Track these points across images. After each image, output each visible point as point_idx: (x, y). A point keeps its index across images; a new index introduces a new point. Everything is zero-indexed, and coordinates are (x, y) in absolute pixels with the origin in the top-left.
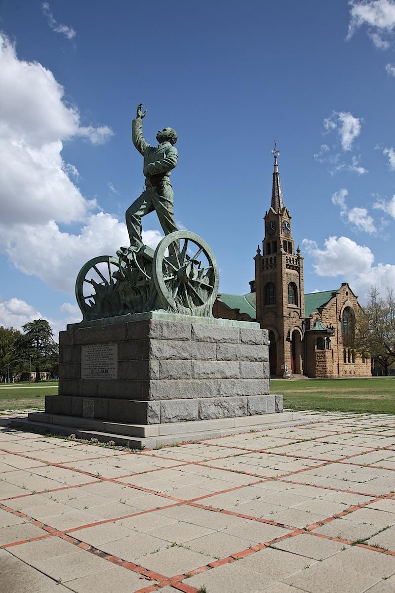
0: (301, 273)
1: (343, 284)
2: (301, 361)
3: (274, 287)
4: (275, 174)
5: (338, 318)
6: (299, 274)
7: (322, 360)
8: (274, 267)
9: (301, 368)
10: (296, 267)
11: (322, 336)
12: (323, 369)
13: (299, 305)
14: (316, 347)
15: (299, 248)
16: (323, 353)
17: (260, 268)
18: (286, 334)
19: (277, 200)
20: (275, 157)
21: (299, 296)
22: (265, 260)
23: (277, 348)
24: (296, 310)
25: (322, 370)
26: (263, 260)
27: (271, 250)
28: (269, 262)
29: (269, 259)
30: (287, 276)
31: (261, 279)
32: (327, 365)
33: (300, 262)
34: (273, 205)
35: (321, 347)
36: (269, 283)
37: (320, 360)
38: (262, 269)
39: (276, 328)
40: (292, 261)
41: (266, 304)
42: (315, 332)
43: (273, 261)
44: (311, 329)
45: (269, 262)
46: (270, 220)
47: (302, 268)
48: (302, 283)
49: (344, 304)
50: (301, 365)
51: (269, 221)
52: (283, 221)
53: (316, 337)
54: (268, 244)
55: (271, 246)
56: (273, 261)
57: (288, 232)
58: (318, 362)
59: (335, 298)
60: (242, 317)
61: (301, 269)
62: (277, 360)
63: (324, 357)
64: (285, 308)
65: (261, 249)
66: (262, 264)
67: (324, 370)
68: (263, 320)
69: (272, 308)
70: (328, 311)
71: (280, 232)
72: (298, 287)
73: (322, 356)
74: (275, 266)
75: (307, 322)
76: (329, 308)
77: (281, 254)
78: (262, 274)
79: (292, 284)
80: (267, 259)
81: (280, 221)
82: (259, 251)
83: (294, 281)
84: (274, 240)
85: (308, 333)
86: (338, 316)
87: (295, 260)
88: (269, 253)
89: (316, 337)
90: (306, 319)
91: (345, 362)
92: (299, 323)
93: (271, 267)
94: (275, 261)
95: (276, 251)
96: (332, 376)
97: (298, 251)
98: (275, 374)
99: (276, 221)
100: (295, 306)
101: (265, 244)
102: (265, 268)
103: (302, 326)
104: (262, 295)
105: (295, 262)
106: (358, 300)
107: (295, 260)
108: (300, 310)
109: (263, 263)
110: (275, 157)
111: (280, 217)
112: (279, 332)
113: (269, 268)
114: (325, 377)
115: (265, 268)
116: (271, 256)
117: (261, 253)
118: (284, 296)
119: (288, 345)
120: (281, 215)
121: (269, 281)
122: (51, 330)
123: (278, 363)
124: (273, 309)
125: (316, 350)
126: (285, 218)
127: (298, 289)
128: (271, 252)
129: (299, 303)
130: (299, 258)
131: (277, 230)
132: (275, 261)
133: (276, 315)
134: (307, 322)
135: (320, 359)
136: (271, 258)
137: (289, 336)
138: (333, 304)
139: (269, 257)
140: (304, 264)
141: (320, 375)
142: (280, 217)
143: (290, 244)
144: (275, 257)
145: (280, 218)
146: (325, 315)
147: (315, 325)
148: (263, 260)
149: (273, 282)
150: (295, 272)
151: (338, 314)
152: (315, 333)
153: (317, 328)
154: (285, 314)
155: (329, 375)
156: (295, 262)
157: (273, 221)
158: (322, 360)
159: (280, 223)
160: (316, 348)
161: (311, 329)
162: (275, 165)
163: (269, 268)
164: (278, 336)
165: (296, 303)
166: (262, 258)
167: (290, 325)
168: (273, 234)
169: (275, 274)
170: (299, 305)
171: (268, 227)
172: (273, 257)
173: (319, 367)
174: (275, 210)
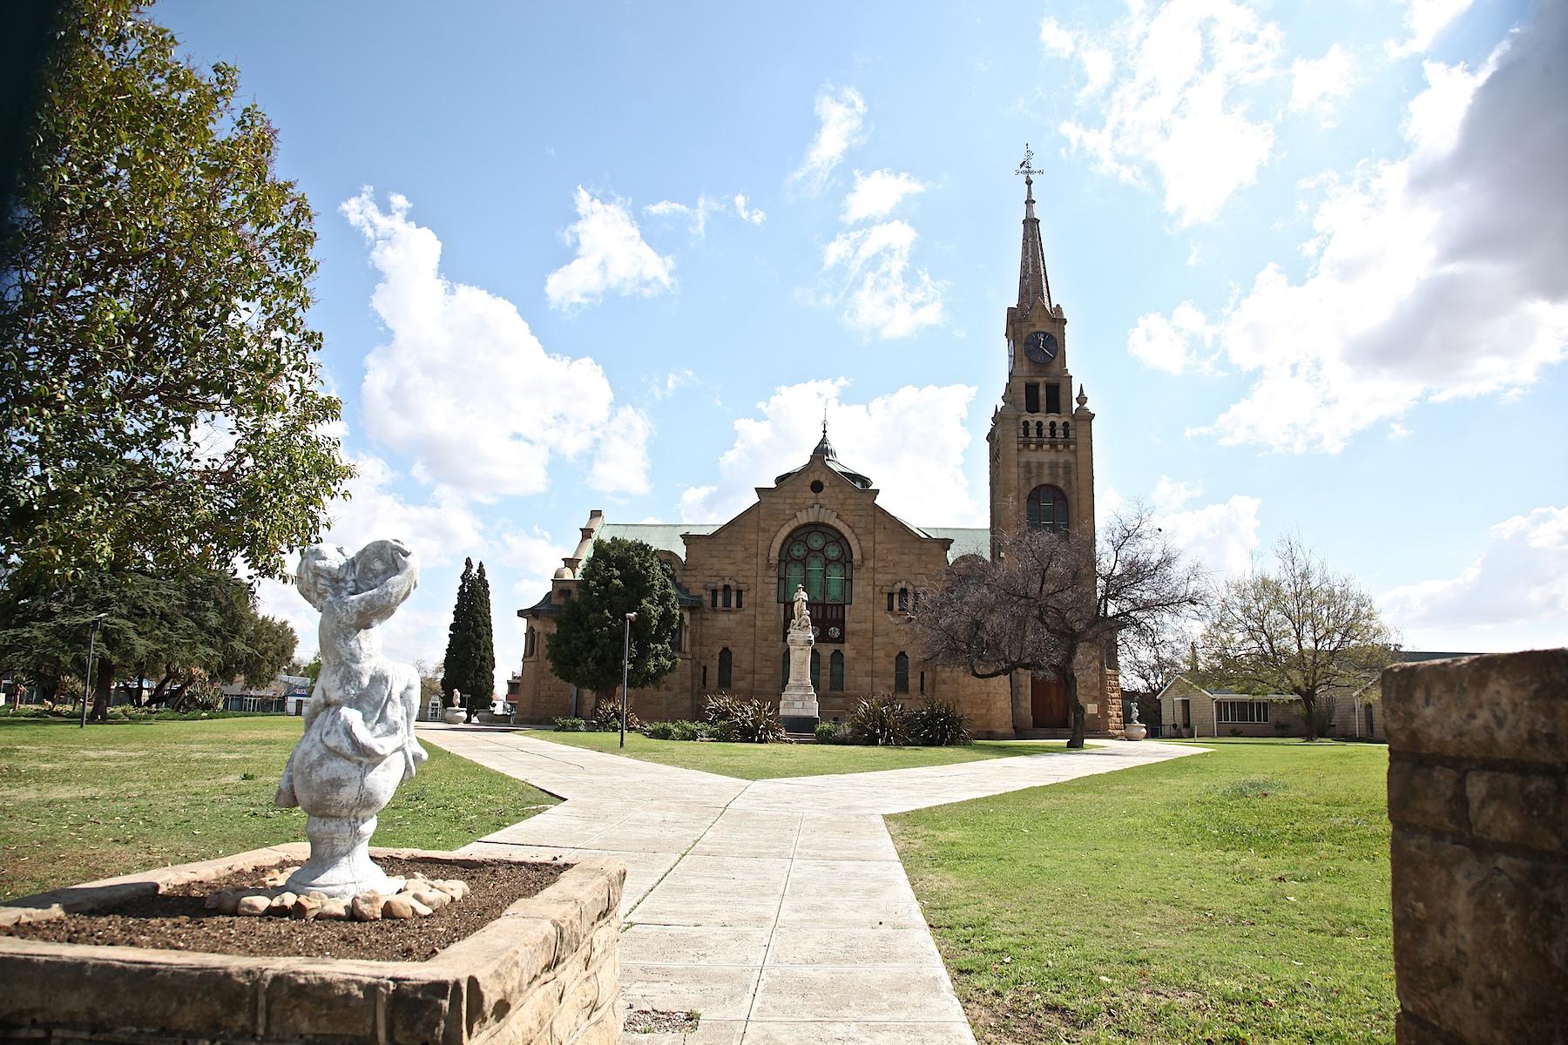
8: (1060, 447)
22: (1033, 425)
27: (1043, 403)
28: (1046, 432)
31: (1022, 471)
38: (1021, 446)
43: (1060, 433)
45: (1046, 432)
46: (1037, 329)
54: (1031, 389)
55: (1042, 392)
56: (1060, 433)
74: (1067, 446)
80: (1053, 424)
84: (1051, 380)
88: (1033, 407)
94: (1066, 434)
99: (1056, 336)
109: (1026, 433)
115: (1032, 446)
121: (1046, 480)
131: (1058, 358)
132: (1066, 434)
144: (1066, 424)
149: (1061, 484)
157: (1045, 334)
163: (1046, 447)
172: (1046, 423)
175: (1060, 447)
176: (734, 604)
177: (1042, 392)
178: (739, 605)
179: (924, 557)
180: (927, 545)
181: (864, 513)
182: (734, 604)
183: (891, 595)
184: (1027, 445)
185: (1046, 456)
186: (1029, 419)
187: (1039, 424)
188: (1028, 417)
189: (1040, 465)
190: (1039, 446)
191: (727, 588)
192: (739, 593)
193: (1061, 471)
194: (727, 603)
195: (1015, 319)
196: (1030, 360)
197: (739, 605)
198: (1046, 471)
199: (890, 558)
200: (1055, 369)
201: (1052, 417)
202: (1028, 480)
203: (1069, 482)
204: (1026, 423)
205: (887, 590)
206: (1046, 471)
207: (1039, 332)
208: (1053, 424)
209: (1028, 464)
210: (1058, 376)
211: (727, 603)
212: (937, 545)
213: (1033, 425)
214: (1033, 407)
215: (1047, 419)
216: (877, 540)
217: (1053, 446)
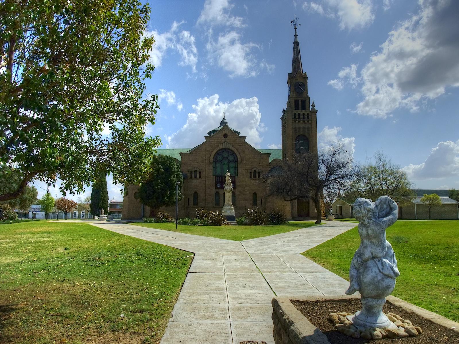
4: (296, 44)
17: (292, 120)
22: (297, 114)
27: (300, 106)
28: (302, 117)
38: (293, 121)
43: (306, 117)
45: (302, 117)
46: (298, 81)
51: (297, 81)
54: (296, 102)
55: (300, 103)
56: (306, 117)
66: (293, 116)
74: (308, 121)
80: (304, 114)
109: (295, 117)
115: (297, 122)
116: (298, 112)
121: (302, 133)
149: (306, 134)
163: (302, 122)
175: (306, 122)
176: (198, 176)
177: (300, 103)
178: (200, 177)
180: (263, 156)
182: (198, 176)
183: (251, 173)
184: (295, 121)
185: (302, 125)
186: (296, 112)
187: (299, 114)
188: (296, 112)
189: (299, 128)
190: (299, 121)
191: (196, 171)
192: (200, 173)
193: (306, 130)
194: (196, 176)
195: (291, 78)
196: (296, 92)
197: (200, 177)
199: (250, 160)
201: (303, 112)
204: (295, 114)
205: (249, 171)
207: (299, 82)
208: (304, 114)
211: (196, 176)
213: (297, 114)
214: (297, 108)
215: (302, 112)
217: (304, 121)
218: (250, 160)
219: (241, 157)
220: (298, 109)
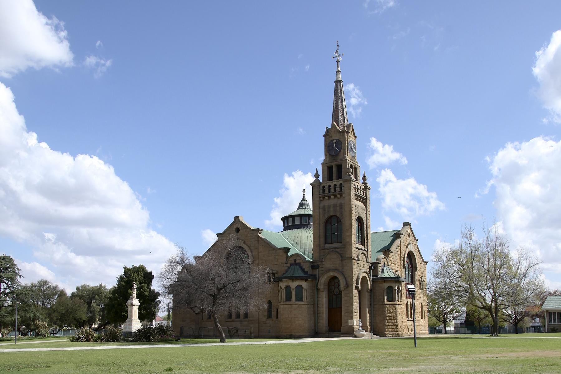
0: (368, 207)
1: (405, 224)
2: (368, 315)
3: (339, 221)
4: (338, 83)
5: (402, 265)
6: (366, 206)
7: (393, 314)
8: (339, 196)
9: (368, 324)
10: (363, 199)
11: (392, 285)
12: (394, 325)
13: (366, 246)
14: (386, 297)
15: (366, 175)
16: (394, 306)
17: (320, 197)
18: (355, 281)
19: (340, 114)
20: (338, 62)
21: (365, 235)
22: (327, 187)
23: (343, 299)
24: (364, 252)
25: (393, 327)
26: (324, 187)
28: (332, 190)
29: (332, 186)
30: (356, 209)
31: (321, 210)
32: (398, 321)
33: (367, 193)
34: (335, 118)
35: (391, 298)
36: (330, 218)
37: (390, 315)
38: (321, 198)
39: (342, 273)
40: (359, 191)
41: (326, 243)
42: (385, 280)
43: (338, 189)
44: (379, 276)
45: (332, 190)
46: (333, 138)
47: (369, 200)
48: (368, 218)
49: (407, 248)
50: (368, 320)
52: (349, 141)
53: (386, 285)
54: (330, 169)
55: (334, 169)
56: (338, 189)
57: (354, 154)
58: (389, 316)
59: (399, 240)
60: (295, 258)
61: (368, 201)
62: (343, 314)
63: (395, 311)
64: (354, 249)
65: (320, 173)
66: (321, 191)
67: (395, 327)
68: (324, 263)
69: (335, 248)
70: (394, 254)
71: (347, 154)
72: (365, 223)
73: (393, 310)
74: (341, 195)
75: (374, 267)
76: (395, 252)
77: (350, 180)
78: (322, 205)
79: (359, 219)
80: (330, 186)
81: (346, 139)
82: (317, 176)
83: (362, 216)
84: (337, 163)
85: (376, 280)
86: (402, 262)
87: (362, 189)
89: (386, 285)
90: (373, 264)
91: (408, 317)
92: (367, 266)
93: (335, 196)
95: (340, 176)
96: (403, 334)
97: (364, 179)
98: (340, 332)
99: (341, 140)
100: (362, 247)
101: (326, 168)
102: (327, 198)
103: (370, 272)
104: (322, 231)
105: (362, 192)
106: (418, 244)
107: (362, 189)
108: (367, 252)
110: (338, 62)
111: (346, 134)
112: (345, 278)
113: (332, 197)
114: (396, 335)
115: (327, 198)
116: (334, 183)
117: (320, 178)
118: (353, 234)
119: (356, 293)
120: (348, 133)
121: (332, 214)
122: (18, 269)
123: (344, 318)
124: (338, 250)
125: (387, 302)
126: (351, 138)
127: (365, 226)
128: (334, 177)
129: (366, 244)
130: (366, 188)
131: (342, 151)
133: (342, 257)
134: (374, 267)
135: (391, 313)
136: (335, 185)
137: (357, 284)
138: (398, 247)
139: (332, 184)
140: (371, 195)
141: (391, 333)
142: (346, 134)
143: (356, 169)
144: (341, 184)
145: (346, 136)
146: (391, 260)
147: (383, 271)
148: (324, 187)
150: (361, 204)
151: (402, 259)
152: (385, 282)
153: (387, 274)
154: (354, 256)
155: (400, 332)
156: (362, 192)
157: (336, 140)
158: (393, 314)
159: (346, 142)
160: (386, 300)
161: (379, 276)
162: (338, 72)
163: (332, 197)
164: (345, 283)
165: (362, 244)
166: (323, 185)
167: (359, 270)
168: (337, 155)
169: (341, 206)
170: (366, 246)
171: (329, 147)
172: (338, 184)
173: (389, 323)
174: (338, 125)
177: (334, 169)
179: (277, 257)
180: (278, 251)
181: (254, 240)
184: (324, 198)
185: (333, 201)
186: (325, 185)
188: (330, 183)
189: (329, 207)
193: (338, 208)
195: (328, 134)
196: (330, 154)
198: (332, 209)
199: (264, 258)
200: (341, 157)
202: (324, 214)
203: (341, 213)
206: (332, 209)
207: (333, 140)
208: (330, 186)
209: (324, 207)
210: (341, 160)
212: (282, 251)
214: (330, 178)
216: (259, 251)
217: (335, 196)
218: (264, 258)
219: (252, 255)
220: (333, 180)
